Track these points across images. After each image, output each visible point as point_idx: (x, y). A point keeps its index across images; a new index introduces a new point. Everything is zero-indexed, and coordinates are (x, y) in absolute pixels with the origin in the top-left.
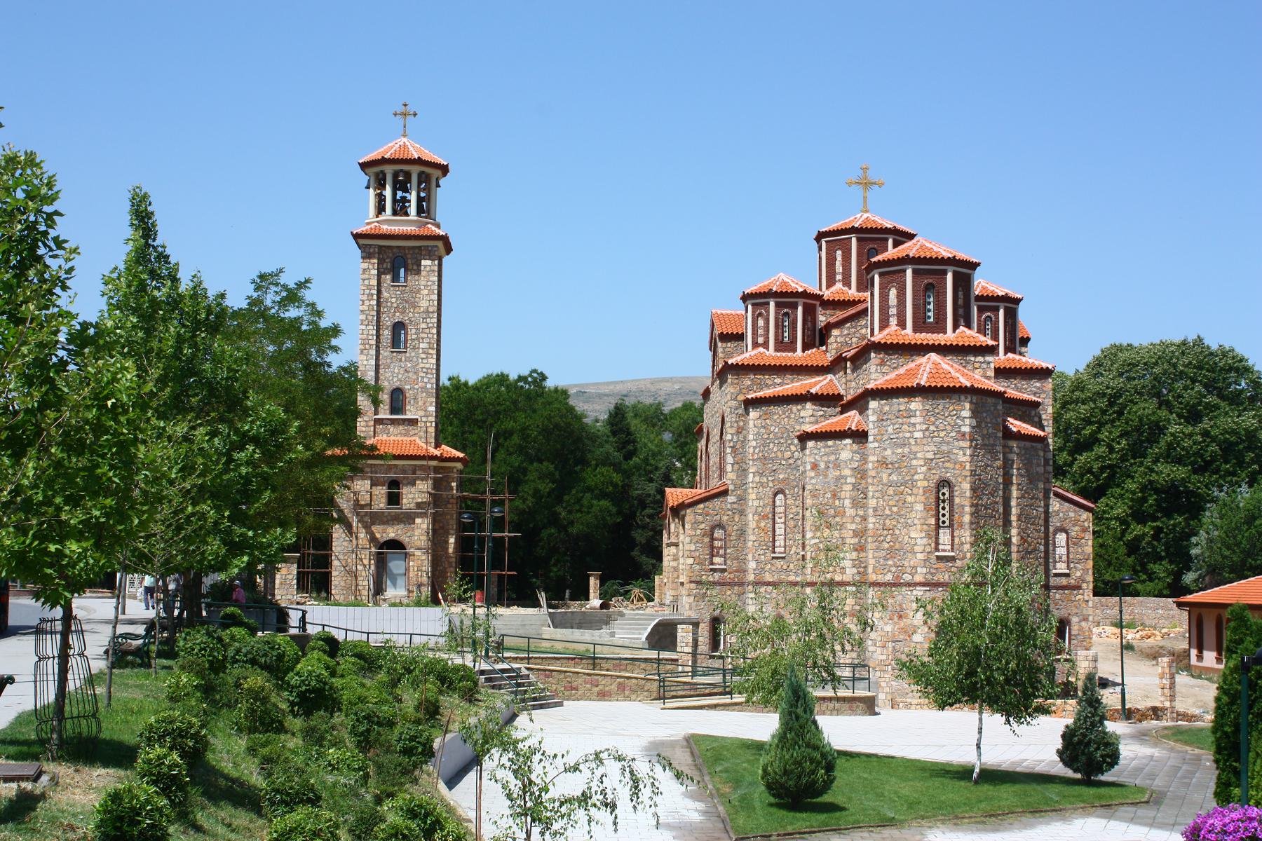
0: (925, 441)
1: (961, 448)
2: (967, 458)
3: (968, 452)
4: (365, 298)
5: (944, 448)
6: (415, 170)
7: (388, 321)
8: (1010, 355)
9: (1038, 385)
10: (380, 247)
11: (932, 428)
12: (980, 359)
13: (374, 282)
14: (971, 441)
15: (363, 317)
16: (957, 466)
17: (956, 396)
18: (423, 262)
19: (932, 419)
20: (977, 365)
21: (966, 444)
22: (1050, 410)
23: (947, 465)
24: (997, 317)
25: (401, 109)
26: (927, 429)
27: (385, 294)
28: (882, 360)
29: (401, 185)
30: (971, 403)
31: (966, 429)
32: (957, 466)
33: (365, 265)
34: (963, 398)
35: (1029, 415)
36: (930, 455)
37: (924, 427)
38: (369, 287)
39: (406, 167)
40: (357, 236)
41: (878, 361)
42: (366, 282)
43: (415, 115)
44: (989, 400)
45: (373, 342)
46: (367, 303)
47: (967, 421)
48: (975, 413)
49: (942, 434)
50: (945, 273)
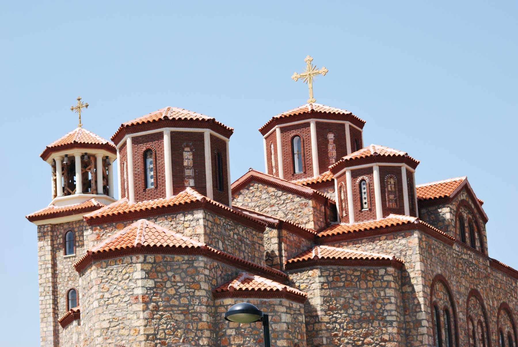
0: (100, 310)
1: (135, 312)
2: (142, 322)
3: (142, 315)
4: (42, 272)
5: (119, 314)
6: (77, 153)
7: (62, 290)
8: (392, 216)
9: (403, 241)
10: (53, 226)
11: (107, 295)
12: (189, 217)
13: (49, 257)
14: (146, 303)
15: (41, 289)
16: (132, 332)
17: (128, 259)
18: (85, 233)
19: (107, 286)
20: (186, 224)
21: (140, 307)
22: (418, 266)
23: (122, 332)
24: (372, 179)
25: (76, 104)
26: (103, 297)
27: (60, 267)
28: (98, 235)
29: (69, 170)
30: (144, 262)
31: (139, 291)
32: (132, 332)
33: (41, 243)
34: (134, 259)
35: (376, 276)
36: (106, 325)
37: (99, 295)
38: (45, 262)
39: (69, 152)
40: (32, 219)
41: (95, 237)
42: (43, 258)
43: (87, 106)
44: (178, 258)
45: (51, 310)
46: (44, 276)
47: (140, 283)
48: (149, 274)
49: (116, 300)
50: (160, 136)
